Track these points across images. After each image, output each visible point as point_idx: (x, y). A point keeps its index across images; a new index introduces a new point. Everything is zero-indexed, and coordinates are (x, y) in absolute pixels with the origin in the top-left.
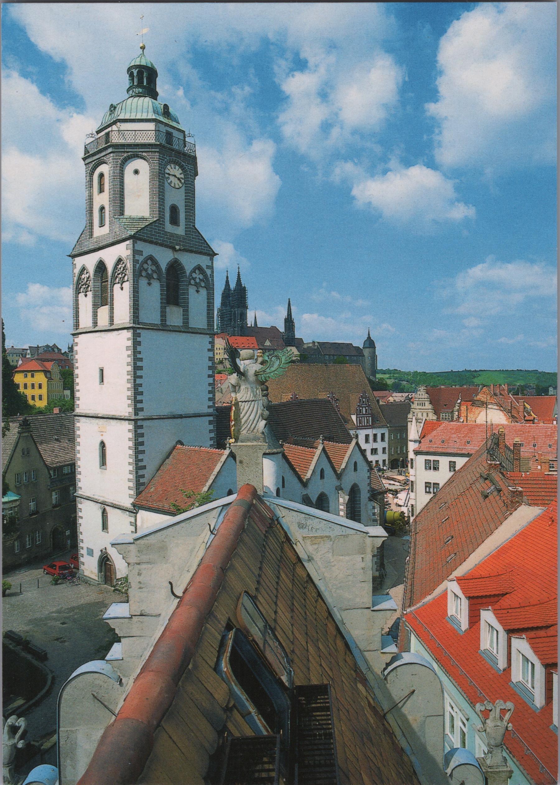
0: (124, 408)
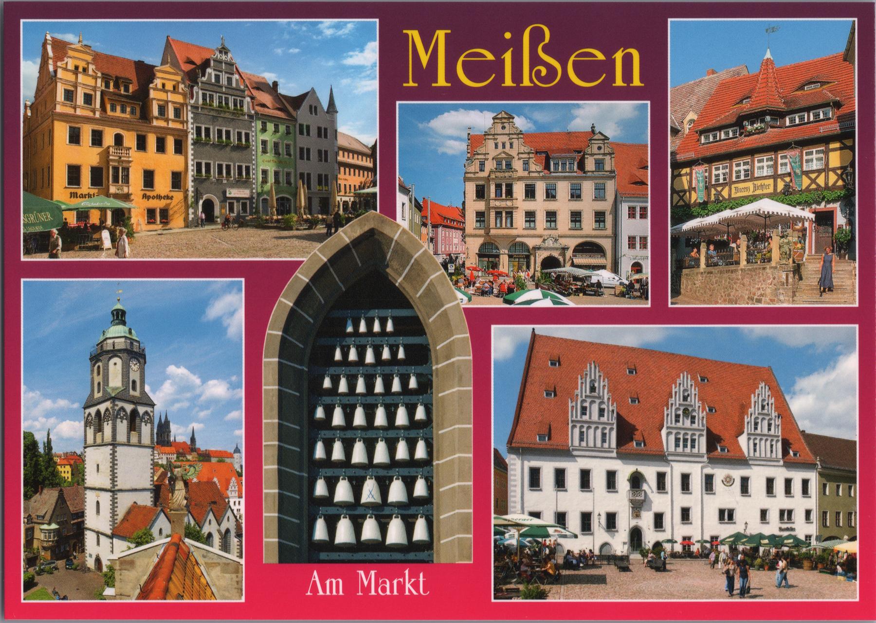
0: (107, 485)
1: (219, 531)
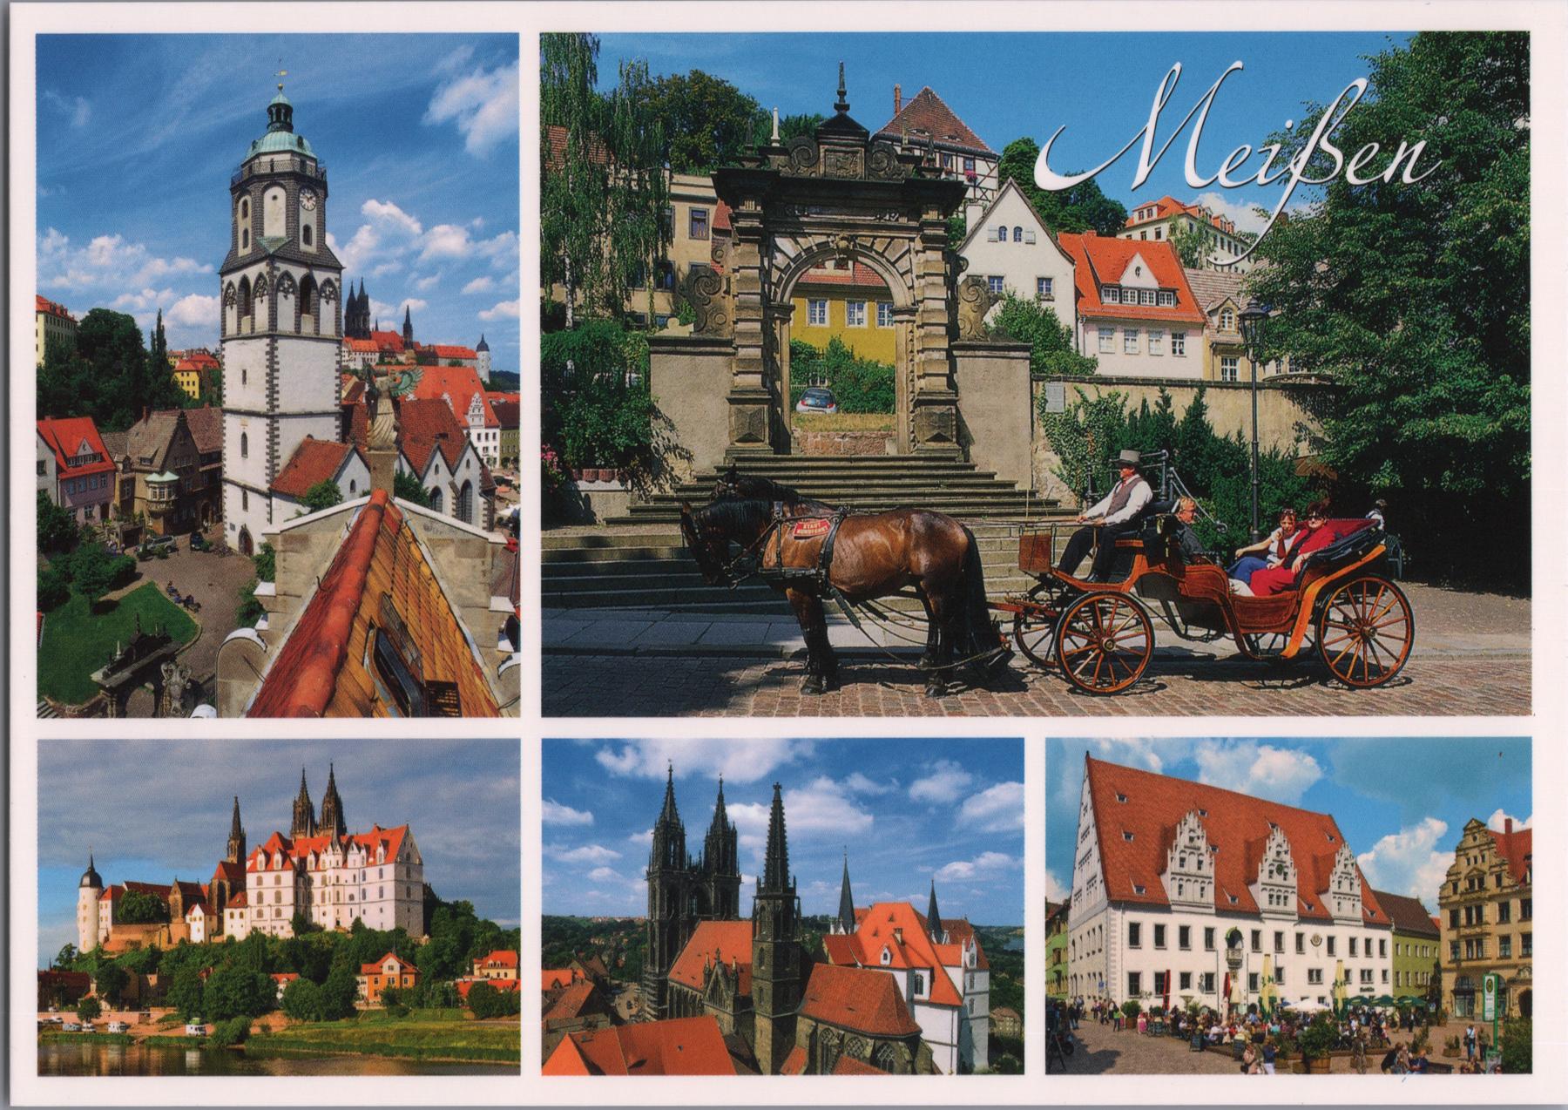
0: (261, 405)
1: (453, 485)
